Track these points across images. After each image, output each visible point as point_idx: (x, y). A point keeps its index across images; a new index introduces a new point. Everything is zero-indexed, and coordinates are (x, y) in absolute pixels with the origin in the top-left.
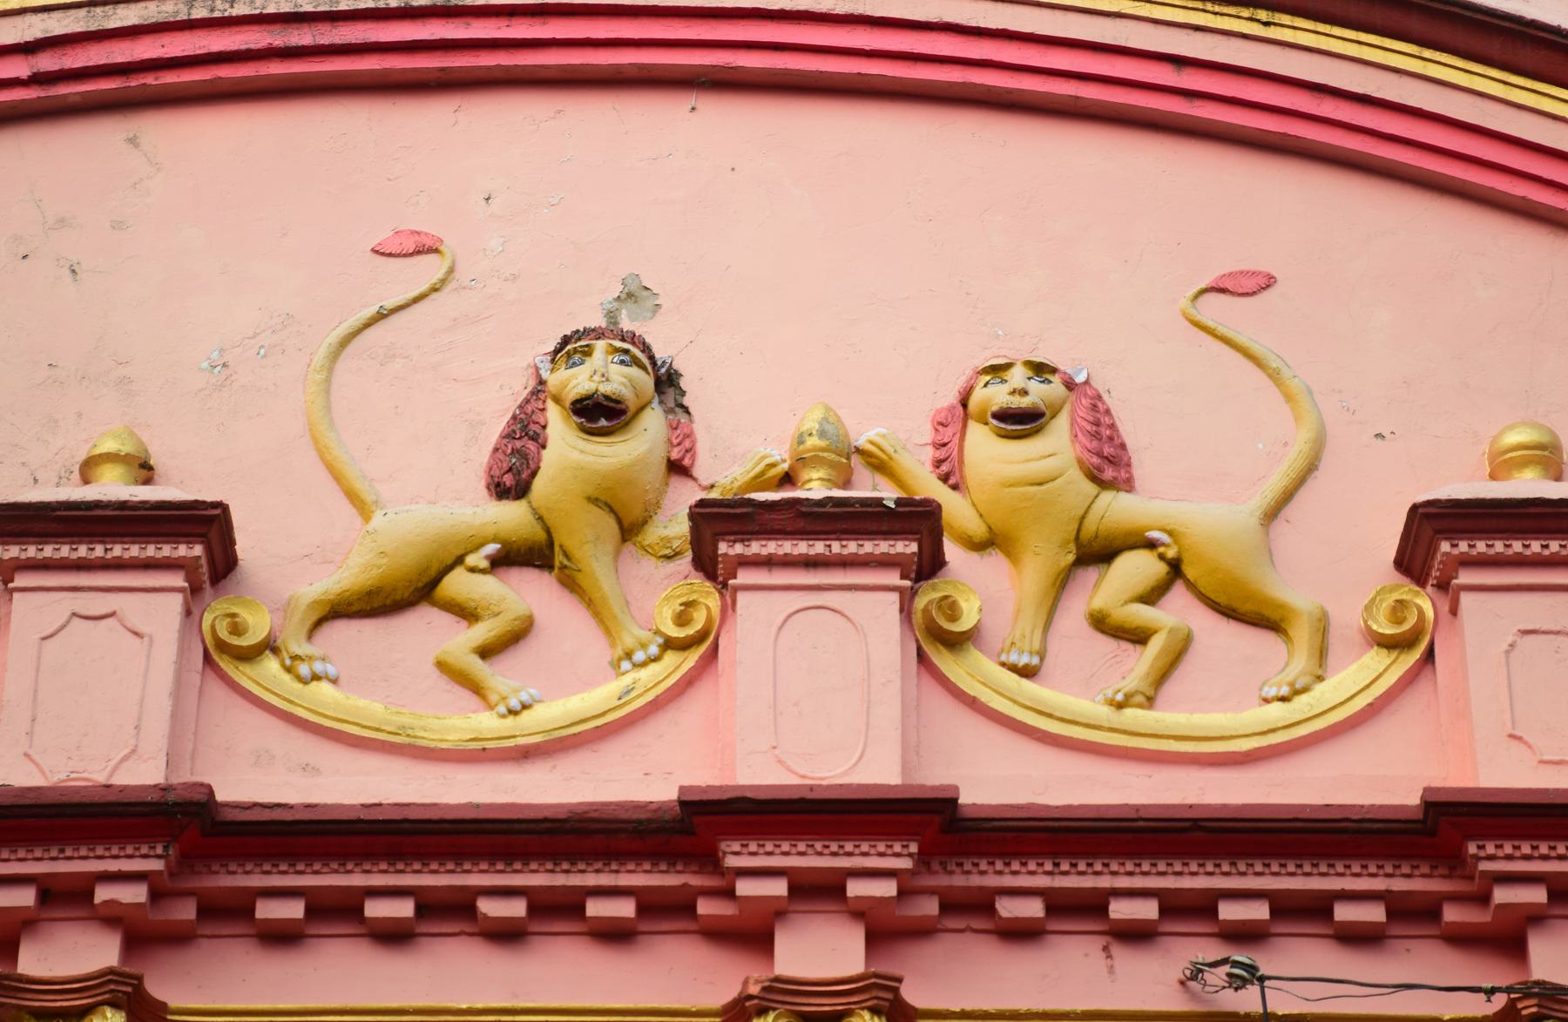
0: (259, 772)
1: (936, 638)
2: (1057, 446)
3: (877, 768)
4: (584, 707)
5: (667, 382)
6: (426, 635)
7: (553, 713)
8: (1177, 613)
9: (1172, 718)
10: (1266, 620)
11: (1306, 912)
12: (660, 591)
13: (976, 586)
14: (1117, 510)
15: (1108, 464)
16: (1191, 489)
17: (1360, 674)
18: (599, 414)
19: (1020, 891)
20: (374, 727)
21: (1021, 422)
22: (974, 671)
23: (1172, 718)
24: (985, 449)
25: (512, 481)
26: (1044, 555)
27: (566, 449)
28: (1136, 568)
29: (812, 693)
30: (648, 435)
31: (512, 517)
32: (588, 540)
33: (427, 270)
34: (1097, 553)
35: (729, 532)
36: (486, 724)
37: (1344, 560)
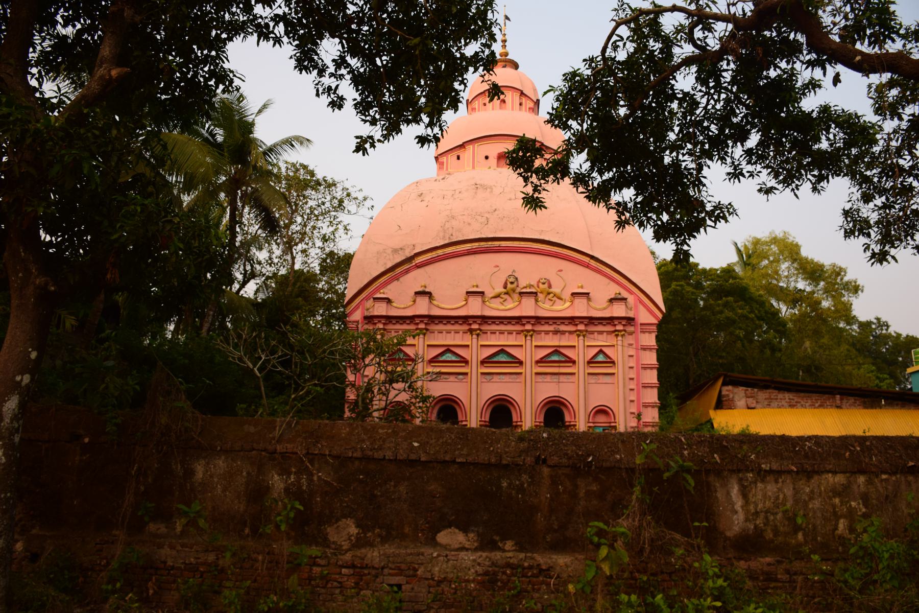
0: (488, 313)
1: (537, 301)
2: (546, 285)
3: (532, 314)
4: (510, 307)
5: (517, 279)
6: (499, 300)
7: (508, 307)
8: (555, 298)
9: (554, 308)
10: (561, 299)
11: (563, 323)
12: (516, 296)
13: (541, 297)
14: (551, 290)
15: (550, 287)
16: (556, 289)
17: (568, 304)
18: (512, 283)
19: (543, 322)
20: (495, 309)
21: (544, 283)
22: (540, 304)
23: (554, 308)
24: (541, 285)
25: (505, 287)
26: (545, 294)
27: (509, 286)
28: (552, 295)
29: (527, 308)
30: (514, 286)
31: (505, 290)
32: (511, 292)
33: (497, 269)
34: (549, 294)
35: (521, 293)
36: (503, 307)
37: (567, 295)
